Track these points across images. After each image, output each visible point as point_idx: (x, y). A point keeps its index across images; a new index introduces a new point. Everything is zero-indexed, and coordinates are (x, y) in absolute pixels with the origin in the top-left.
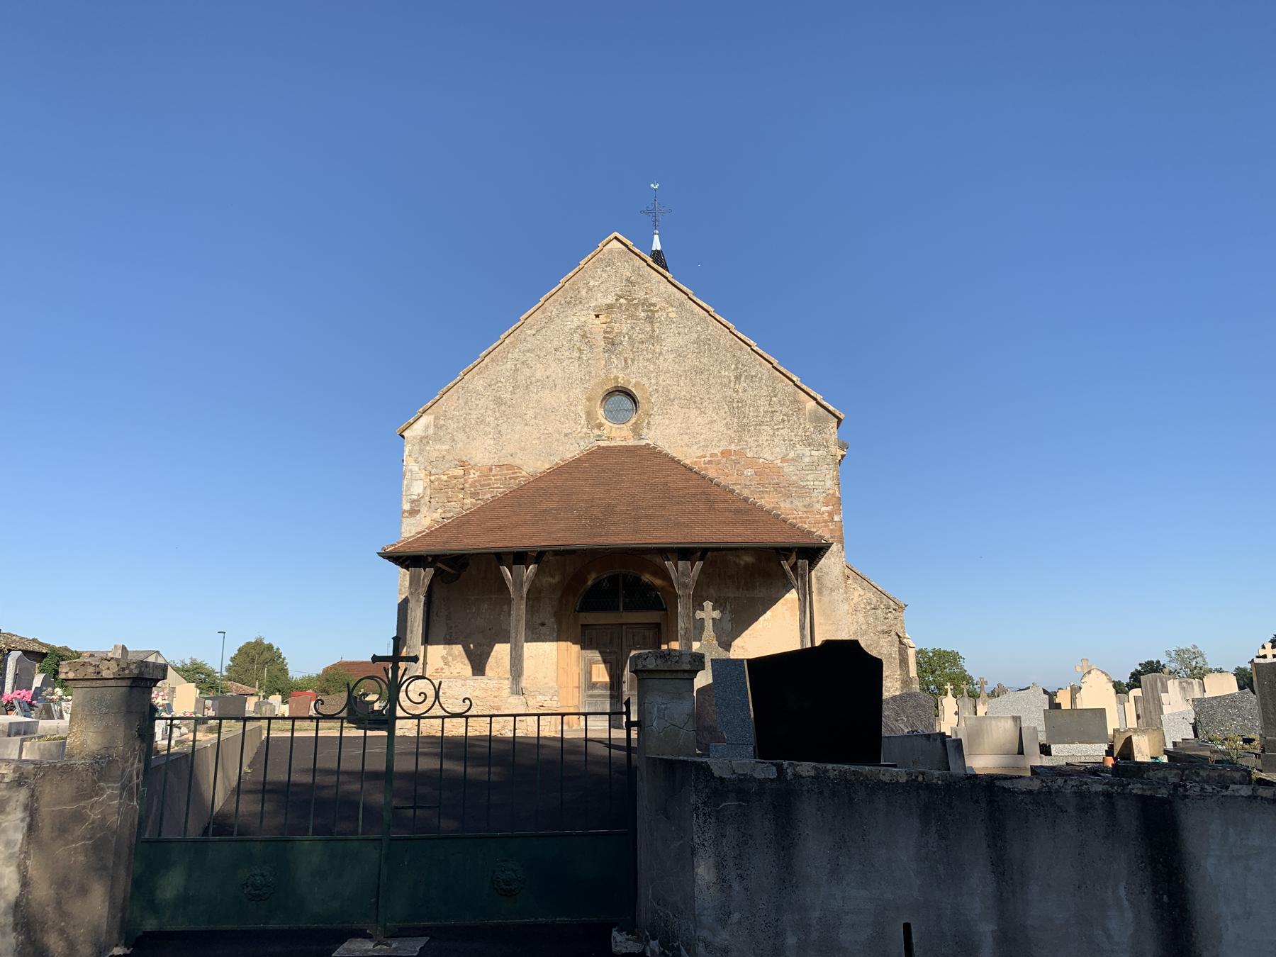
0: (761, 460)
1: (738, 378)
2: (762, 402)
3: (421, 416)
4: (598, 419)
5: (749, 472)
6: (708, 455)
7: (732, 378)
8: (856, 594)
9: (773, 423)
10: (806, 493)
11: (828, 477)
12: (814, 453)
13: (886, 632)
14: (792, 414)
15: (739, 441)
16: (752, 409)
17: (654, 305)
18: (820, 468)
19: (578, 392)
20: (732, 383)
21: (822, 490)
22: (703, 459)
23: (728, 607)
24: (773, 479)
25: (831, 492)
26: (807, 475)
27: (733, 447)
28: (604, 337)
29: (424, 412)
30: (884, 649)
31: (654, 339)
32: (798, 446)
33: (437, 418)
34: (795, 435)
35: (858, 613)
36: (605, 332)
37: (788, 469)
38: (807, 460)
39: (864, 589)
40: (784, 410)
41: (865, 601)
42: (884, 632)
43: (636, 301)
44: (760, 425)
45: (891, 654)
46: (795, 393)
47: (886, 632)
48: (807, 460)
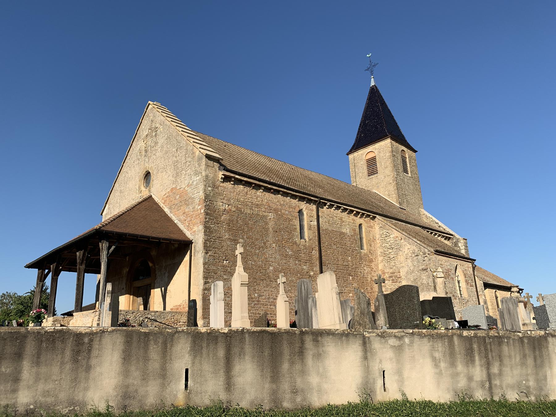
0: (182, 189)
1: (177, 150)
2: (183, 159)
3: (105, 206)
4: (141, 188)
5: (178, 197)
6: (167, 193)
7: (175, 151)
8: (406, 248)
9: (186, 168)
10: (194, 201)
11: (201, 189)
12: (198, 178)
13: (425, 270)
14: (192, 161)
15: (176, 182)
16: (180, 163)
17: (157, 128)
18: (199, 185)
19: (137, 179)
20: (175, 153)
21: (198, 198)
22: (165, 196)
23: (167, 270)
24: (184, 197)
25: (201, 197)
26: (195, 191)
27: (174, 186)
28: (145, 150)
29: (106, 204)
30: (424, 281)
31: (156, 143)
32: (192, 177)
33: (109, 205)
34: (192, 171)
35: (408, 260)
36: (145, 148)
37: (189, 190)
38: (195, 183)
39: (410, 244)
40: (189, 159)
41: (411, 251)
42: (424, 270)
43: (153, 129)
44: (182, 171)
45: (428, 283)
46: (193, 149)
47: (425, 270)
48: (195, 183)
